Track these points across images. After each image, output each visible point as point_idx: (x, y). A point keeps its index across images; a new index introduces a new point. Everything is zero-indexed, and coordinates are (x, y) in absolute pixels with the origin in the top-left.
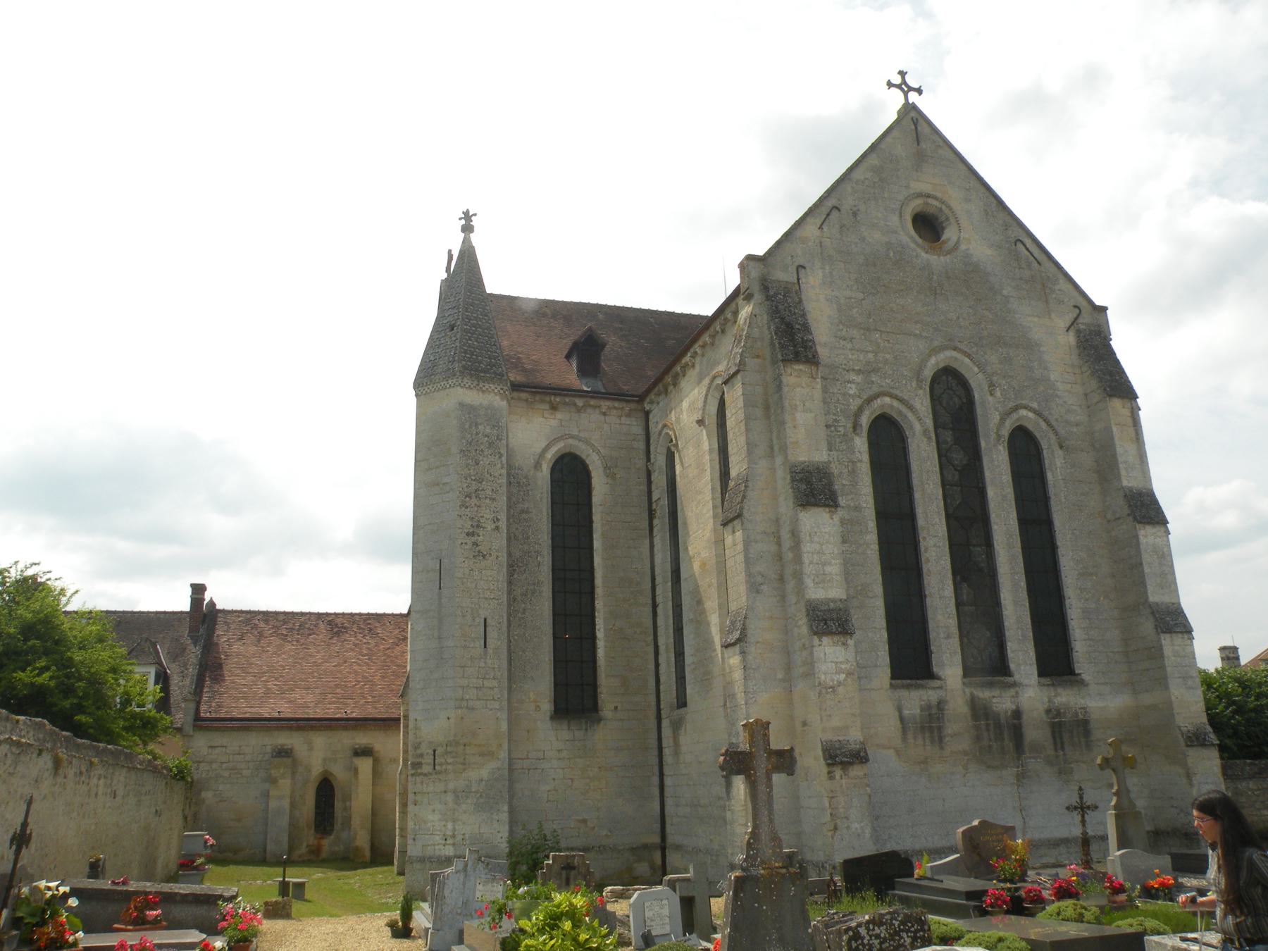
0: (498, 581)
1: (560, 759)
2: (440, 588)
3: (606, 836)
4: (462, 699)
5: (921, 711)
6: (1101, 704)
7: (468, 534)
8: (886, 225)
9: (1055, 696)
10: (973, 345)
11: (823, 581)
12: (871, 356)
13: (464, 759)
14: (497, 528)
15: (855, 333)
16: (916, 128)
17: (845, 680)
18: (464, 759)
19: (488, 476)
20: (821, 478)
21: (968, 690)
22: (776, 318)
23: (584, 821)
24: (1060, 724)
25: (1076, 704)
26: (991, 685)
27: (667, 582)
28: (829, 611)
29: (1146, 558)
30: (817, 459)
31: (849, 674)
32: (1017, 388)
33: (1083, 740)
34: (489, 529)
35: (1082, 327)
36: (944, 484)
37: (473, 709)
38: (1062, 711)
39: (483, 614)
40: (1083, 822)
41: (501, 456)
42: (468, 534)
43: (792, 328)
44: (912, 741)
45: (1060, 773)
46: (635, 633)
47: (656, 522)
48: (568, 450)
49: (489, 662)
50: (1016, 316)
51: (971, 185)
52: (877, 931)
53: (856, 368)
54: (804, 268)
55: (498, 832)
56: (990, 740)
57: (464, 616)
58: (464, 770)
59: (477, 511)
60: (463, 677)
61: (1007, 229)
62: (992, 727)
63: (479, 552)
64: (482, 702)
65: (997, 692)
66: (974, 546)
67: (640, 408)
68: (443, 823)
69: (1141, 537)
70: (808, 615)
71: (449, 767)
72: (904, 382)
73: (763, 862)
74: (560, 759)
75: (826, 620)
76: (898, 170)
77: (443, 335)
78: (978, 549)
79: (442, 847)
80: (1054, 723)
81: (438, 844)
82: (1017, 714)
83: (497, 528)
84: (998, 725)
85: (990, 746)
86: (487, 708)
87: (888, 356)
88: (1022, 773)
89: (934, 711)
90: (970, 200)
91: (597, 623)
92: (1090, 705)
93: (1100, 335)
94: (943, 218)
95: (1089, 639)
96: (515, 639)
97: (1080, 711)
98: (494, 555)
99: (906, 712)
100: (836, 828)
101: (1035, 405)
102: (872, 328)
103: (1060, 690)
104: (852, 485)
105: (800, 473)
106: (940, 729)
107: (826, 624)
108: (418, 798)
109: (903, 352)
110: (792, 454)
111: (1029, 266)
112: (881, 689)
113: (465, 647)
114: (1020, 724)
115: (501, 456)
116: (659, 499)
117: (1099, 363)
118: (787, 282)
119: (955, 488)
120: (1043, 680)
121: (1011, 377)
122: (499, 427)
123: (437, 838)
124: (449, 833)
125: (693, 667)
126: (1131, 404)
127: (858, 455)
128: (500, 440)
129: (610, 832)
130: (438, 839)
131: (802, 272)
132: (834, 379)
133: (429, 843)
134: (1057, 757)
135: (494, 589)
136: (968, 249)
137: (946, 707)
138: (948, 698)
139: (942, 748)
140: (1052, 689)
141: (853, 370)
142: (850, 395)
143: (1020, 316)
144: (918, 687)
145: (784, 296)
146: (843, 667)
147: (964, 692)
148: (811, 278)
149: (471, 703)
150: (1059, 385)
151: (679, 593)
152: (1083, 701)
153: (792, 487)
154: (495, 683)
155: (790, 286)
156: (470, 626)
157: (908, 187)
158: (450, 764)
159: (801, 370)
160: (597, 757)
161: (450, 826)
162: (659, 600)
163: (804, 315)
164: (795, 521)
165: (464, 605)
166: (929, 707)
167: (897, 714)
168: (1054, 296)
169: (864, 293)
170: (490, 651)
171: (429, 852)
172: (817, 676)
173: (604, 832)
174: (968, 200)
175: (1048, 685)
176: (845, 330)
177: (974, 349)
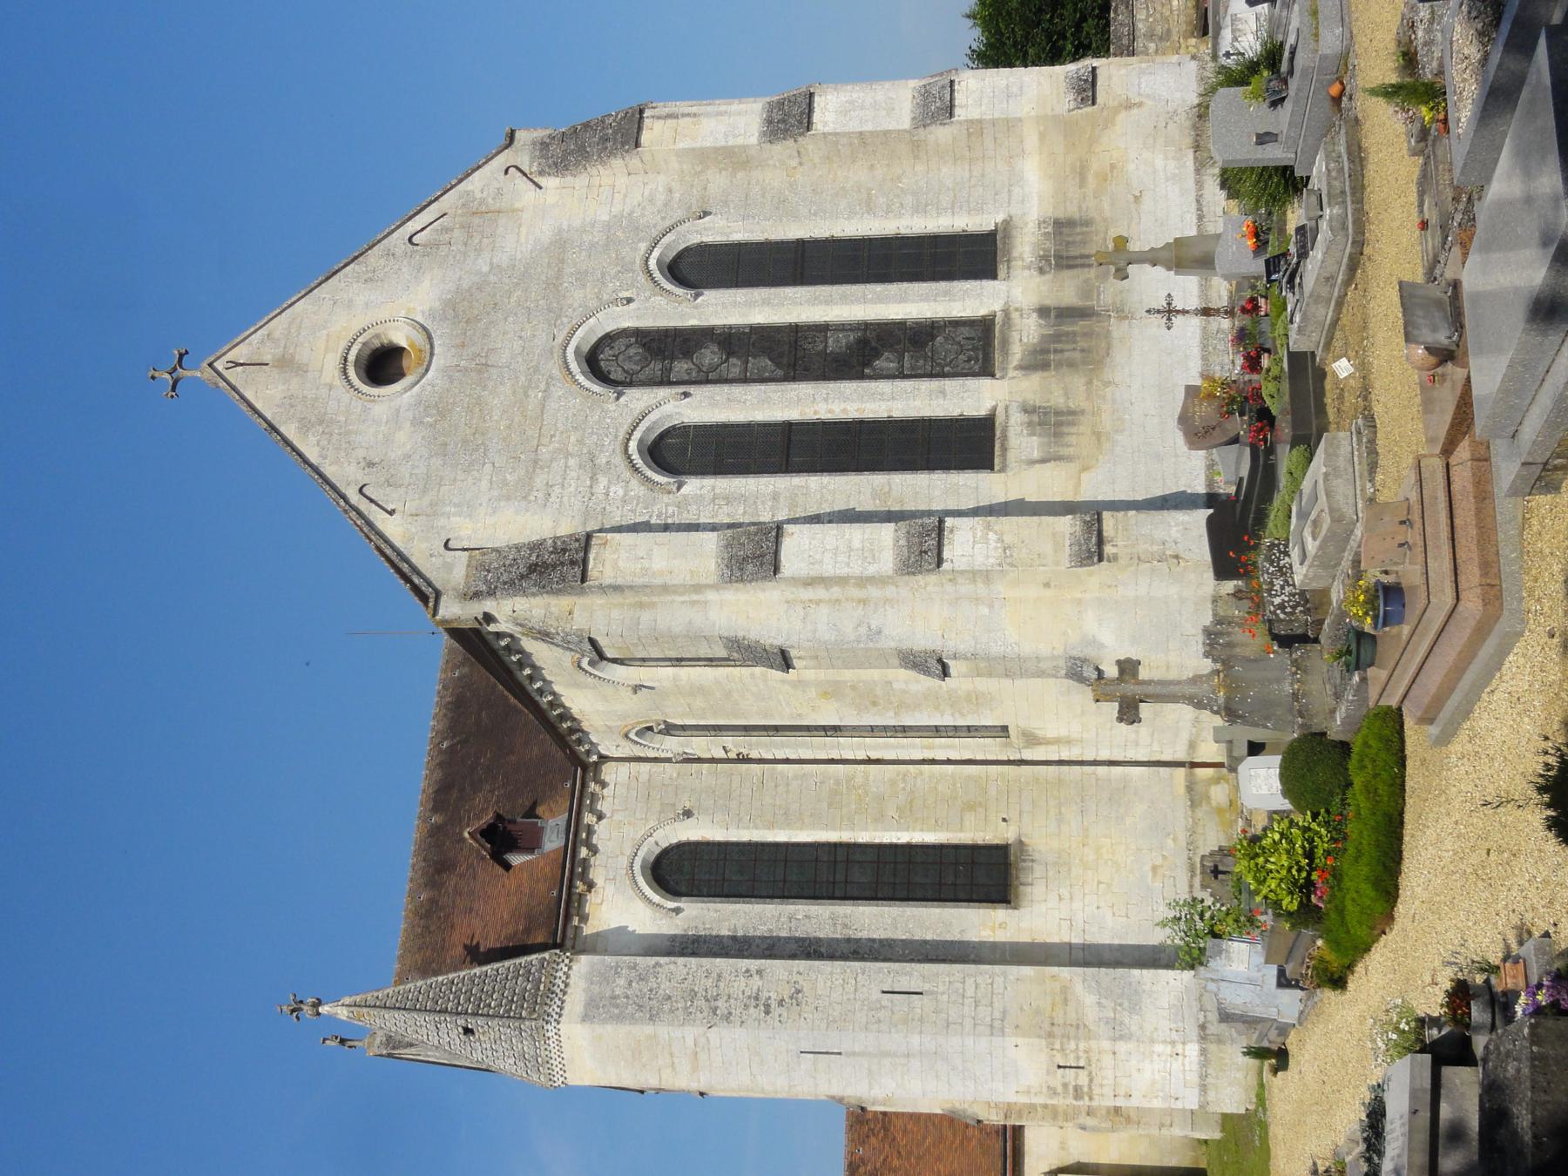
0: (831, 973)
1: (1071, 898)
2: (840, 1054)
3: (1174, 840)
4: (992, 1026)
5: (1035, 435)
6: (1035, 201)
7: (767, 1013)
8: (387, 422)
11: (872, 550)
12: (572, 462)
13: (1071, 1025)
14: (759, 972)
15: (539, 481)
16: (242, 365)
17: (996, 533)
18: (1071, 1025)
19: (686, 982)
20: (740, 544)
21: (1011, 373)
22: (521, 585)
23: (1155, 869)
24: (1058, 257)
25: (1033, 233)
26: (1005, 343)
27: (839, 743)
28: (909, 547)
29: (854, 126)
30: (714, 547)
31: (988, 527)
32: (619, 268)
33: (1078, 230)
34: (760, 983)
35: (534, 169)
36: (744, 380)
37: (1004, 1012)
38: (1041, 253)
39: (876, 995)
40: (1184, 312)
41: (657, 964)
42: (767, 1013)
43: (536, 565)
44: (1071, 451)
46: (904, 789)
47: (754, 755)
48: (649, 872)
49: (941, 989)
50: (519, 257)
51: (328, 296)
52: (1277, 587)
53: (588, 483)
54: (448, 540)
55: (1168, 983)
56: (1074, 349)
57: (880, 1021)
58: (1085, 1026)
59: (736, 999)
60: (962, 1024)
61: (393, 255)
62: (1059, 346)
63: (791, 998)
64: (995, 1000)
65: (1015, 336)
66: (826, 346)
67: (591, 768)
68: (1155, 1056)
69: (826, 130)
70: (914, 574)
71: (1082, 1046)
72: (609, 421)
73: (1213, 693)
74: (1071, 898)
75: (921, 552)
77: (478, 1044)
78: (830, 342)
79: (1187, 1061)
80: (1057, 265)
81: (1183, 1065)
82: (1043, 311)
83: (759, 972)
84: (1057, 338)
85: (1083, 351)
86: (1003, 994)
87: (573, 439)
89: (1035, 418)
90: (351, 301)
91: (888, 841)
92: (1036, 217)
93: (548, 145)
94: (377, 344)
95: (953, 207)
96: (910, 953)
97: (1043, 230)
98: (795, 977)
99: (1036, 455)
100: (1177, 557)
101: (643, 246)
102: (533, 456)
103: (1015, 254)
105: (732, 571)
106: (1057, 413)
107: (926, 552)
108: (1122, 1092)
109: (567, 418)
110: (706, 578)
112: (1005, 483)
113: (921, 1020)
114: (1055, 308)
115: (657, 964)
116: (724, 747)
117: (587, 152)
118: (468, 566)
119: (750, 365)
121: (603, 274)
122: (617, 966)
123: (1175, 1066)
124: (1169, 1049)
125: (957, 715)
127: (704, 491)
128: (636, 964)
129: (1169, 835)
130: (1176, 1065)
131: (451, 544)
132: (603, 515)
133: (1182, 1077)
135: (843, 980)
136: (423, 313)
137: (1031, 402)
138: (1020, 400)
139: (1083, 412)
140: (1013, 263)
141: (591, 487)
142: (625, 495)
143: (518, 253)
144: (1005, 437)
145: (489, 571)
146: (979, 534)
147: (1014, 378)
148: (462, 533)
149: (997, 1015)
150: (616, 210)
151: (854, 728)
153: (750, 582)
154: (970, 982)
155: (474, 563)
156: (893, 1013)
157: (331, 387)
158: (1077, 1046)
159: (594, 559)
160: (1070, 847)
161: (1159, 1048)
162: (861, 756)
163: (518, 548)
164: (795, 581)
165: (864, 1020)
166: (1030, 424)
167: (1037, 466)
169: (484, 464)
170: (926, 987)
171: (1193, 1078)
172: (989, 568)
173: (1170, 842)
175: (1009, 268)
176: (536, 494)
177: (565, 320)
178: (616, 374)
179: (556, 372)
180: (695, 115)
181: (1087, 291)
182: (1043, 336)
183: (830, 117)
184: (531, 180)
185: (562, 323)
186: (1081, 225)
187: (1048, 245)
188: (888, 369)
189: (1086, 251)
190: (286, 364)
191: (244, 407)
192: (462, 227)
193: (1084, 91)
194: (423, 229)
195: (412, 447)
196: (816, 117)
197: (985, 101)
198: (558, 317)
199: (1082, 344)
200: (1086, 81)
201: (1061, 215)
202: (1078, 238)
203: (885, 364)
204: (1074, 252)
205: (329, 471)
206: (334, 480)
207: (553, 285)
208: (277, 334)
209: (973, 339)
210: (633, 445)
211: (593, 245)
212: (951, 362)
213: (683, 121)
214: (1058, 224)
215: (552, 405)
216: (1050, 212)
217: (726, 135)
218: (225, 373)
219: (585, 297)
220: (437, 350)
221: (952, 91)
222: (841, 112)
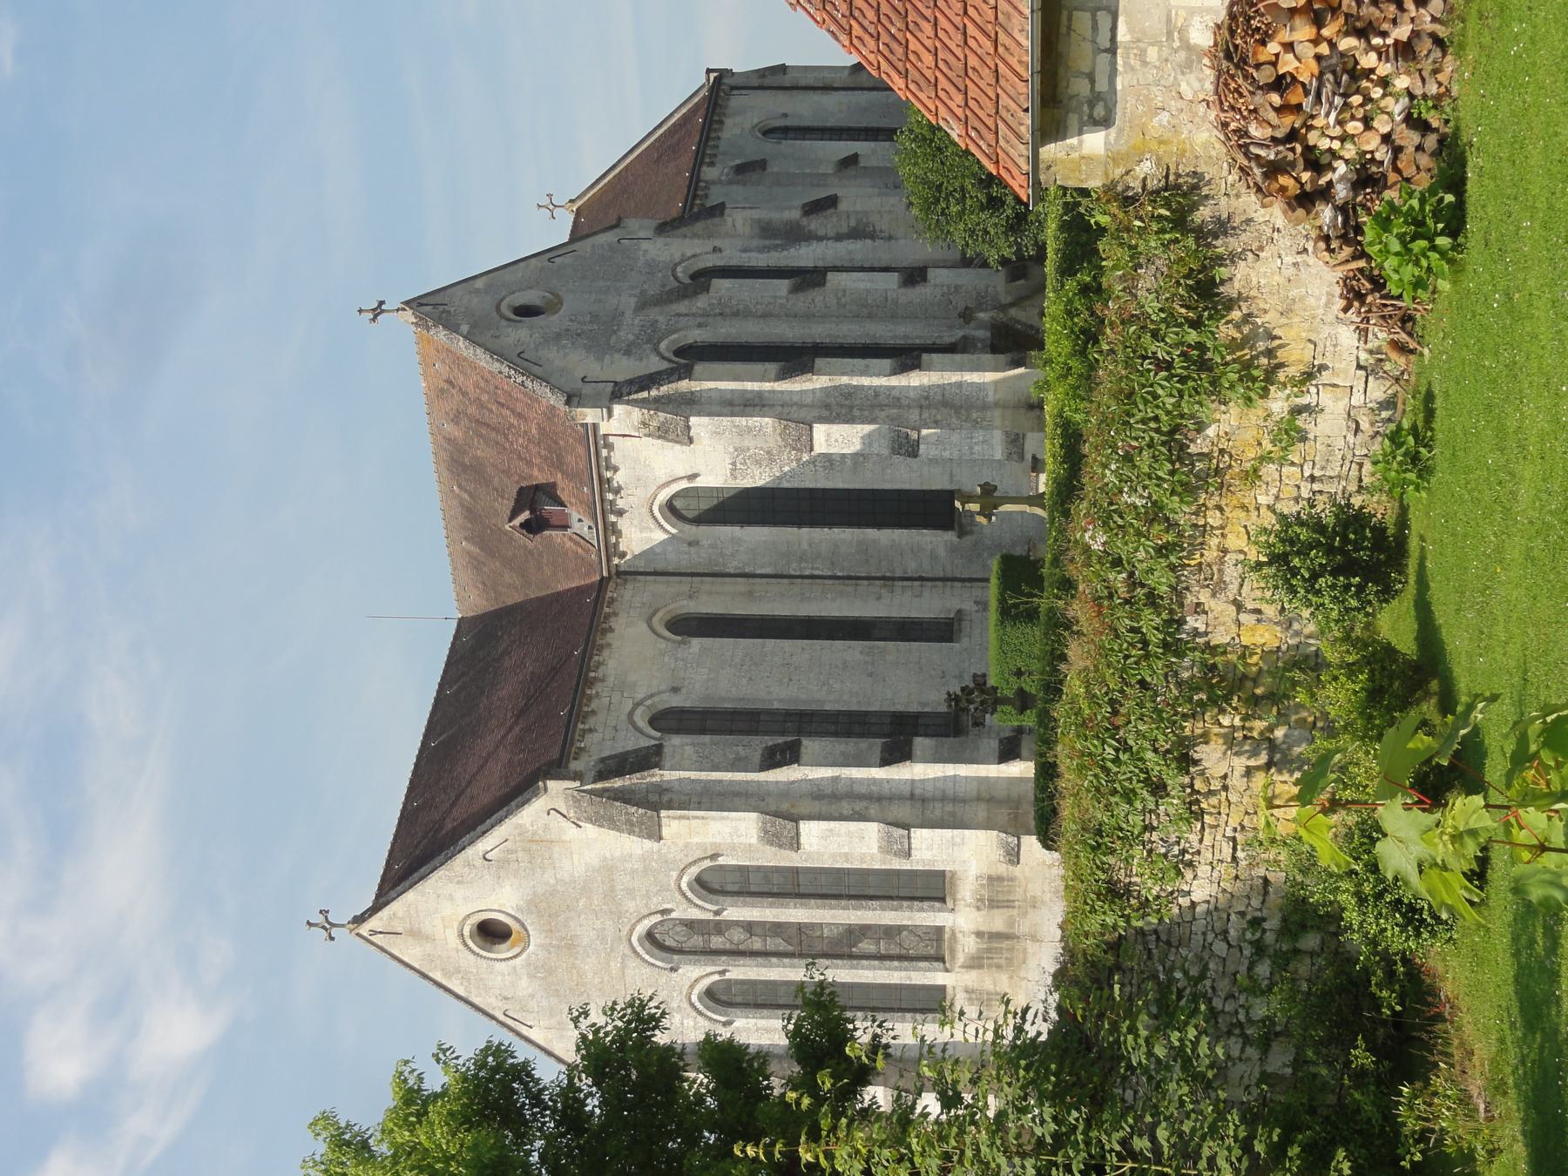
65: (960, 948)
82: (979, 934)
84: (989, 950)
101: (674, 874)
103: (959, 896)
120: (950, 904)
174: (451, 897)
178: (669, 942)
179: (628, 951)
180: (703, 818)
181: (1011, 922)
182: (978, 949)
183: (814, 841)
190: (416, 934)
191: (396, 964)
192: (523, 850)
196: (803, 840)
197: (935, 846)
198: (619, 918)
201: (993, 874)
204: (1001, 897)
205: (477, 1001)
206: (482, 1006)
207: (610, 895)
208: (400, 914)
210: (694, 998)
211: (633, 871)
213: (695, 823)
214: (990, 878)
215: (629, 972)
218: (372, 938)
221: (909, 838)
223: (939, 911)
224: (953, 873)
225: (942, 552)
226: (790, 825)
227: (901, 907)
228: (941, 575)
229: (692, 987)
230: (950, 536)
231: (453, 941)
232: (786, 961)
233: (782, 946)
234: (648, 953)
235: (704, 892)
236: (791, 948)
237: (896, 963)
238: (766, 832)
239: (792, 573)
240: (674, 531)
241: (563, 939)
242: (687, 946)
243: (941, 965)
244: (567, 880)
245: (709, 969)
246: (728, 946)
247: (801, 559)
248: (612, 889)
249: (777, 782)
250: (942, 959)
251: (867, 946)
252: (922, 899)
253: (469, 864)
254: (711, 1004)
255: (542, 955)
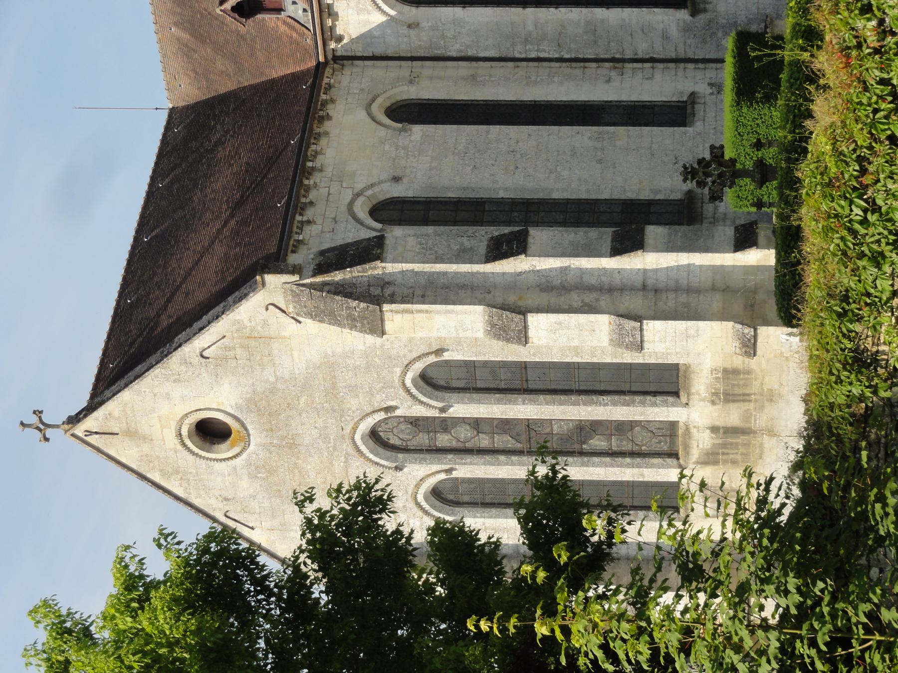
8: (229, 475)
9: (699, 394)
10: (343, 419)
16: (96, 433)
24: (726, 394)
25: (707, 377)
33: (742, 376)
38: (713, 391)
45: (771, 400)
50: (297, 372)
51: (147, 390)
56: (737, 453)
62: (725, 451)
65: (694, 444)
76: (158, 457)
80: (724, 399)
82: (714, 429)
84: (724, 445)
85: (742, 454)
88: (769, 432)
90: (167, 394)
92: (709, 366)
97: (714, 376)
101: (398, 371)
103: (693, 390)
104: (507, 531)
111: (227, 348)
120: (683, 399)
126: (387, 311)
134: (756, 401)
140: (692, 397)
152: (705, 371)
168: (259, 328)
174: (168, 396)
178: (394, 441)
179: (351, 450)
180: (427, 312)
181: (747, 416)
184: (293, 318)
185: (346, 420)
186: (744, 373)
187: (718, 386)
188: (599, 439)
189: (747, 392)
190: (132, 434)
192: (242, 347)
193: (747, 346)
194: (209, 347)
195: (254, 491)
196: (531, 333)
198: (342, 416)
199: (742, 450)
200: (749, 340)
201: (728, 365)
202: (741, 382)
203: (598, 443)
204: (737, 391)
205: (197, 502)
206: (202, 507)
208: (116, 414)
209: (663, 429)
210: (420, 498)
211: (356, 368)
212: (646, 443)
213: (418, 316)
214: (726, 371)
216: (720, 363)
217: (457, 330)
218: (88, 439)
219: (360, 403)
220: (251, 432)
221: (641, 330)
222: (551, 330)
223: (673, 405)
224: (687, 367)
225: (674, 32)
226: (518, 318)
227: (633, 402)
228: (674, 56)
229: (418, 486)
230: (683, 15)
231: (172, 441)
232: (514, 458)
233: (511, 444)
234: (371, 452)
235: (429, 389)
236: (519, 446)
237: (628, 460)
238: (493, 325)
239: (517, 55)
240: (393, 13)
241: (283, 438)
242: (412, 444)
243: (675, 461)
244: (287, 377)
245: (435, 467)
246: (454, 444)
247: (526, 41)
248: (334, 386)
249: (504, 274)
250: (675, 455)
251: (598, 443)
252: (655, 394)
253: (186, 362)
254: (437, 503)
255: (262, 454)
